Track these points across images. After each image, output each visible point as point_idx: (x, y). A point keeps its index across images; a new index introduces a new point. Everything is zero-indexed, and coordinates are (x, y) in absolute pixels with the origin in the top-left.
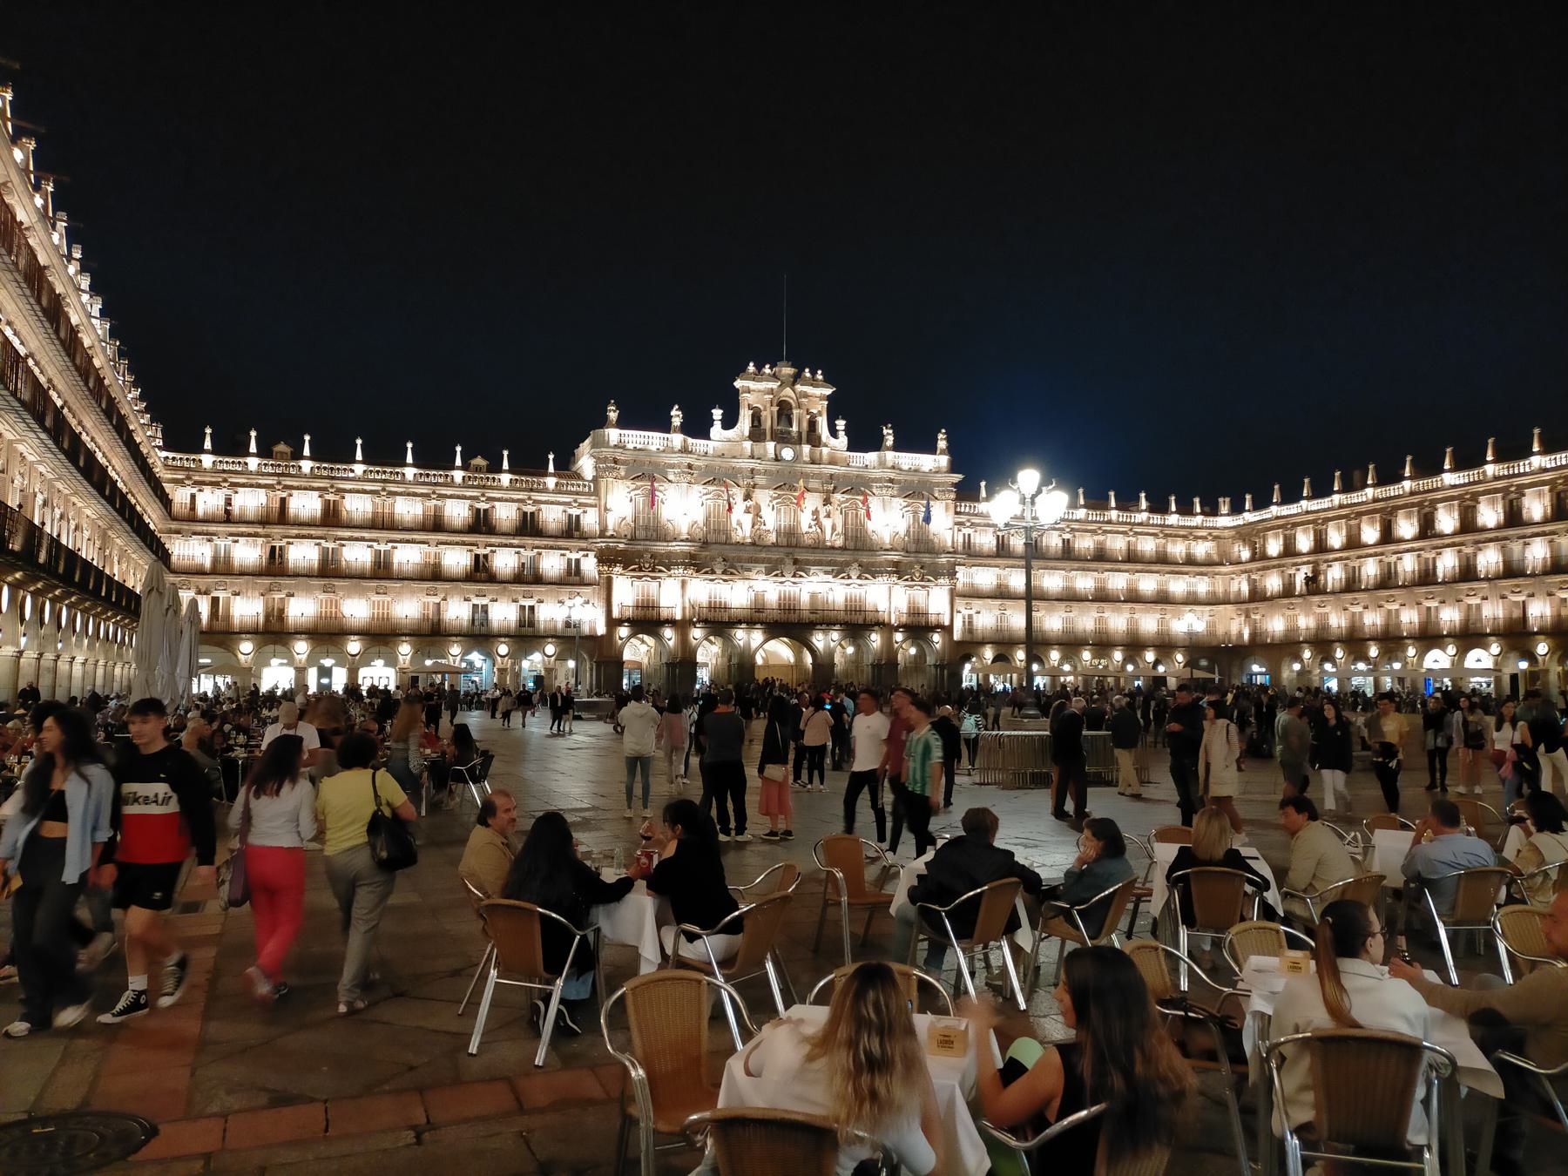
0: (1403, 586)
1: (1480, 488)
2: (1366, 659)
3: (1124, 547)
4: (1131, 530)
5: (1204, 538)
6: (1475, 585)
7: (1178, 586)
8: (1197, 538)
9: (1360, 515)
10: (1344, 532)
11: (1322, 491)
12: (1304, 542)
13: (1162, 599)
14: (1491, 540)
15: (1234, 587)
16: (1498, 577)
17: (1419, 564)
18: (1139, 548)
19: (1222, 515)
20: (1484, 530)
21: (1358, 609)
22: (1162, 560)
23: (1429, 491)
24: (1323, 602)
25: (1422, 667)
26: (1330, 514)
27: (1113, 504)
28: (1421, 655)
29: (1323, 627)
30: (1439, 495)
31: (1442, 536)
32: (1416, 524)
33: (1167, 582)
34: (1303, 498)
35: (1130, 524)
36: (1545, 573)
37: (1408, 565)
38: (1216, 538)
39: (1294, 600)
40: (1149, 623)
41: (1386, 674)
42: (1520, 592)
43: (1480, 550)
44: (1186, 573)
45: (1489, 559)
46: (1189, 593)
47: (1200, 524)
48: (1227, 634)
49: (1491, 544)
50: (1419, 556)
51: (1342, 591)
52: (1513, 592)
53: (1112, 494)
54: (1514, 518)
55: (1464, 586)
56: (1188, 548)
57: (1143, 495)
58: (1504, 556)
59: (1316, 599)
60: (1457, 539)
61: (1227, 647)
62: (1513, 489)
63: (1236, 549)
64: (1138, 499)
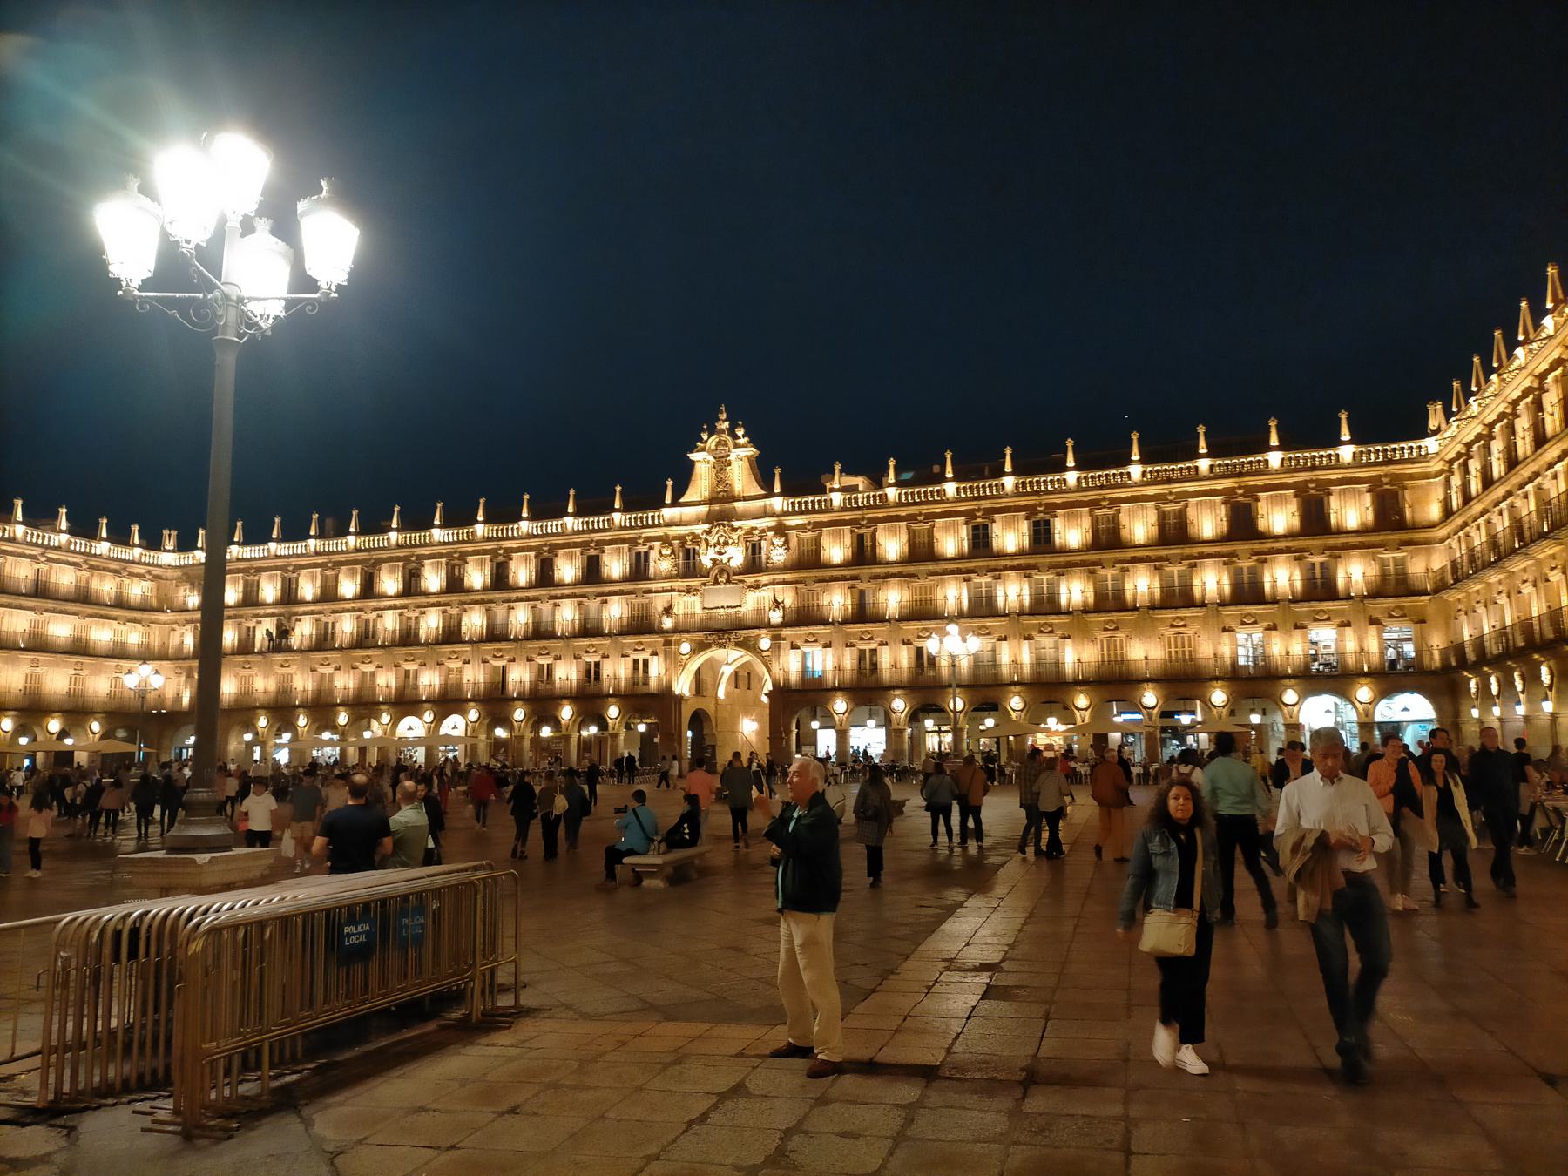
0: (383, 647)
1: (469, 548)
2: (333, 727)
3: (31, 576)
4: (43, 554)
5: (141, 576)
6: (458, 648)
7: (102, 634)
8: (131, 575)
9: (338, 564)
10: (318, 583)
11: (295, 533)
12: (269, 591)
13: (79, 649)
14: (476, 602)
15: (174, 640)
16: (481, 641)
17: (400, 623)
18: (52, 579)
19: (165, 551)
20: (471, 591)
21: (327, 670)
22: (83, 598)
23: (416, 546)
24: (286, 661)
25: (394, 734)
26: (303, 561)
27: (19, 516)
28: (395, 722)
29: (284, 691)
30: (427, 551)
31: (427, 594)
32: (401, 579)
33: (88, 628)
34: (272, 540)
35: (42, 546)
36: (527, 638)
37: (389, 623)
38: (156, 578)
39: (250, 658)
40: (57, 680)
41: (352, 744)
42: (501, 656)
43: (466, 611)
44: (115, 619)
45: (474, 622)
46: (116, 643)
47: (137, 560)
48: (161, 697)
49: (477, 606)
50: (401, 614)
51: (311, 649)
52: (495, 656)
53: (19, 502)
54: (500, 580)
55: (447, 648)
56: (120, 586)
57: (63, 511)
58: (488, 619)
59: (279, 657)
60: (443, 599)
61: (159, 713)
62: (501, 552)
63: (181, 593)
64: (56, 516)
